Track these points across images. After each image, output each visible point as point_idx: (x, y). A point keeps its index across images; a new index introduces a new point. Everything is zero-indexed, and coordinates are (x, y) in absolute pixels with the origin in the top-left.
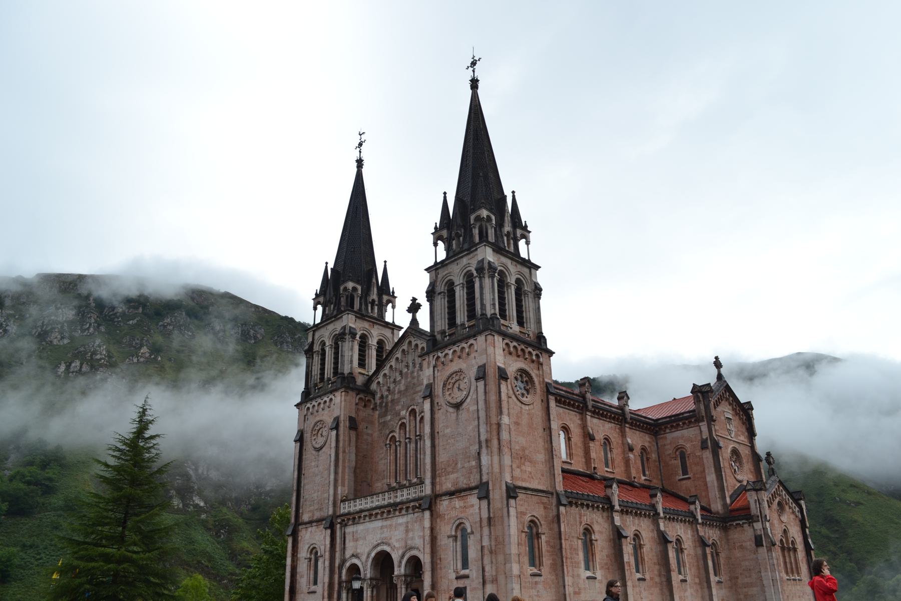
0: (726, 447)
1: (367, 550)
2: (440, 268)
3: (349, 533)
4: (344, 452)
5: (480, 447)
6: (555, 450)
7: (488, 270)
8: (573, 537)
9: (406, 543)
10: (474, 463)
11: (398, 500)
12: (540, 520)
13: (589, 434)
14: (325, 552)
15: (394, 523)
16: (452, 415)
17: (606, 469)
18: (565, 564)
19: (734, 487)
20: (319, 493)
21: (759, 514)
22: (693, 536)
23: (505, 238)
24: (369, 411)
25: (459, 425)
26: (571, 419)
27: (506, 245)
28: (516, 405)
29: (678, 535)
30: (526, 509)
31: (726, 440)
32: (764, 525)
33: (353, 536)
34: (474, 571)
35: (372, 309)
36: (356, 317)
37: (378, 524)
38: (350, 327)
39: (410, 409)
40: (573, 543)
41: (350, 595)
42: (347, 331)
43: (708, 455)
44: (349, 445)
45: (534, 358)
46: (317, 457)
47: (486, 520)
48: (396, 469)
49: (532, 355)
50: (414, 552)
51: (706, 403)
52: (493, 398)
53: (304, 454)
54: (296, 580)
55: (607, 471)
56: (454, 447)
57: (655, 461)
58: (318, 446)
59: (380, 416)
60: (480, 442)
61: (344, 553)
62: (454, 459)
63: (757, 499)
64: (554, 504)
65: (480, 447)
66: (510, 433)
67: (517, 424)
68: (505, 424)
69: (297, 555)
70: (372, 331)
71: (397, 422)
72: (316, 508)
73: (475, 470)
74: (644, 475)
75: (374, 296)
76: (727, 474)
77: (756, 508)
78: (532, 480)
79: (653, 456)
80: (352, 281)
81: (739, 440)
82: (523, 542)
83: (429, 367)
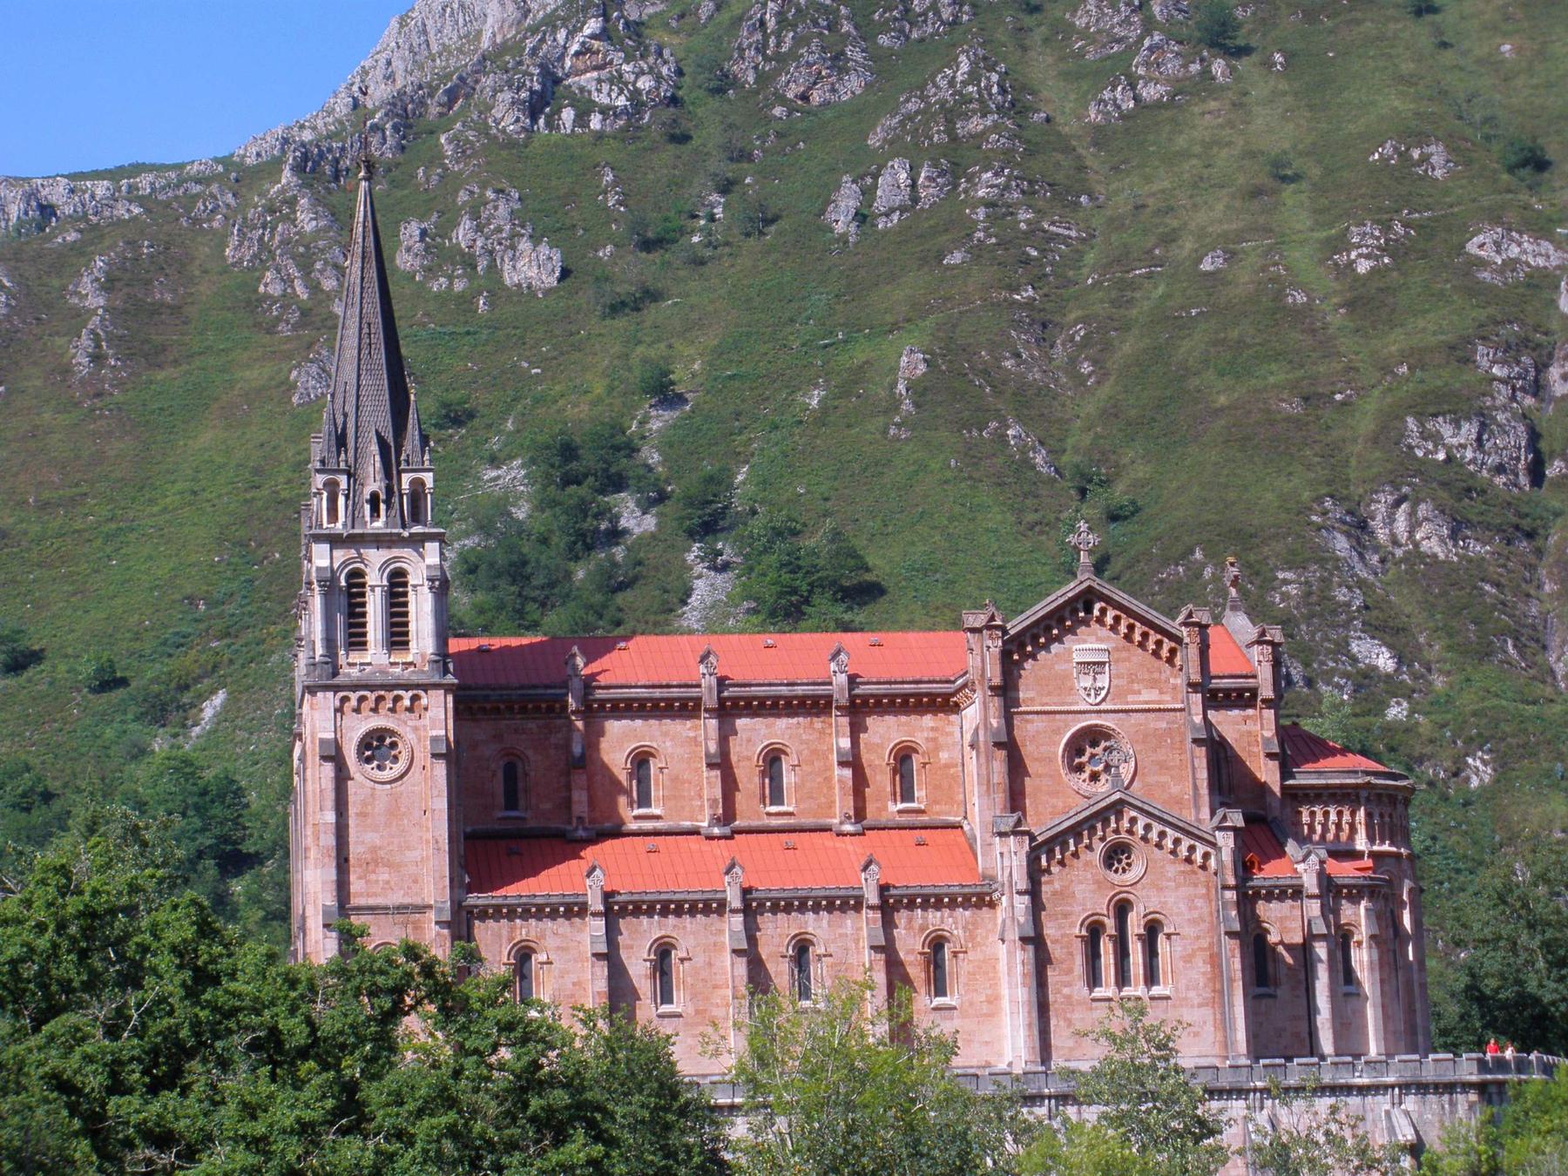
23: (367, 507)
26: (666, 734)
55: (769, 814)
57: (947, 766)
67: (362, 815)
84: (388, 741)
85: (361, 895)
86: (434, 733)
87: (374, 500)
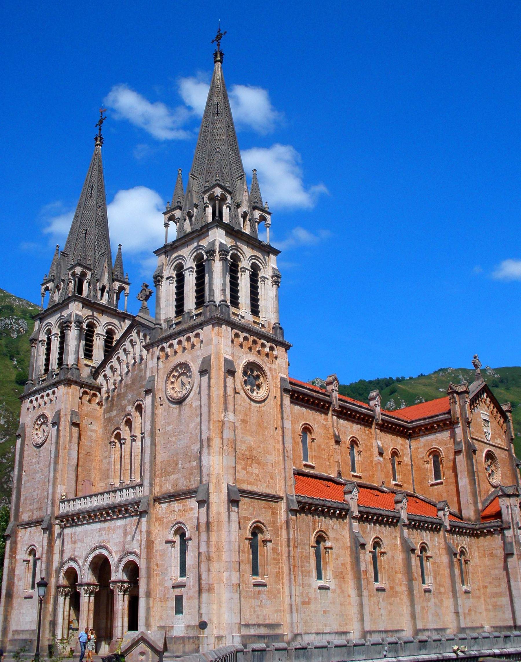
0: (482, 451)
1: (84, 554)
2: (170, 250)
3: (68, 534)
4: (65, 448)
5: (202, 446)
6: (287, 452)
7: (219, 252)
8: (305, 544)
9: (124, 546)
10: (195, 463)
11: (117, 501)
12: (267, 526)
13: (335, 435)
14: (42, 554)
15: (112, 526)
16: (175, 411)
17: (353, 473)
18: (292, 573)
19: (488, 492)
20: (40, 491)
21: (510, 520)
22: (439, 543)
23: (241, 220)
24: (94, 405)
25: (181, 421)
26: (314, 419)
27: (242, 226)
28: (245, 401)
29: (424, 543)
30: (251, 514)
31: (481, 443)
32: (516, 532)
33: (72, 538)
34: (191, 579)
35: (102, 295)
36: (83, 304)
37: (97, 526)
38: (77, 315)
39: (136, 404)
40: (304, 551)
41: (68, 600)
42: (73, 319)
43: (461, 459)
44: (70, 441)
45: (267, 350)
46: (38, 453)
47: (205, 524)
48: (121, 468)
49: (266, 347)
50: (131, 557)
51: (461, 404)
52: (217, 392)
53: (25, 449)
54: (13, 583)
55: (353, 476)
56: (175, 446)
57: (407, 465)
58: (40, 441)
59: (106, 411)
60: (201, 441)
61: (62, 556)
62: (175, 459)
63: (509, 504)
64: (283, 510)
65: (202, 446)
66: (235, 431)
67: (244, 421)
68: (229, 421)
69: (15, 557)
70: (100, 319)
71: (122, 418)
72: (35, 507)
73: (196, 471)
74: (395, 479)
75: (105, 281)
76: (481, 479)
77: (508, 514)
78: (259, 482)
79: (406, 459)
80: (80, 265)
81: (495, 443)
82: (246, 549)
83: (152, 358)
84: (255, 373)
85: (244, 482)
86: (282, 375)
87: (244, 216)
